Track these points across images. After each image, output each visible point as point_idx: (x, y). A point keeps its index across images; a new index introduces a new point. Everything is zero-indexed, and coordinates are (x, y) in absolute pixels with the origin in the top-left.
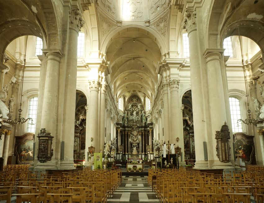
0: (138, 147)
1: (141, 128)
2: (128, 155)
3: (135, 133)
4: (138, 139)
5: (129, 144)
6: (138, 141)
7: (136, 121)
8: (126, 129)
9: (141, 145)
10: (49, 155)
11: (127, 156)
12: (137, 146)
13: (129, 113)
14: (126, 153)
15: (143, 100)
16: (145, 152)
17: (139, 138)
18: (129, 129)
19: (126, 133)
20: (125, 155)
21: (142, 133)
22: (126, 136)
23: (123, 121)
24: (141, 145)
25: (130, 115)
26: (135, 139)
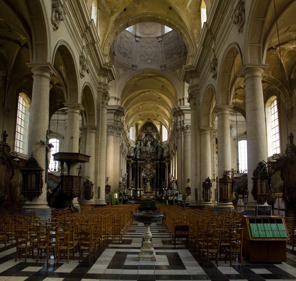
2: (140, 191)
3: (149, 166)
4: (152, 173)
5: (141, 178)
6: (152, 175)
7: (150, 153)
9: (155, 180)
11: (138, 192)
12: (151, 181)
13: (142, 143)
14: (138, 189)
15: (159, 129)
18: (142, 162)
19: (138, 167)
20: (136, 191)
21: (157, 166)
23: (134, 153)
24: (155, 180)
25: (144, 146)
26: (149, 173)
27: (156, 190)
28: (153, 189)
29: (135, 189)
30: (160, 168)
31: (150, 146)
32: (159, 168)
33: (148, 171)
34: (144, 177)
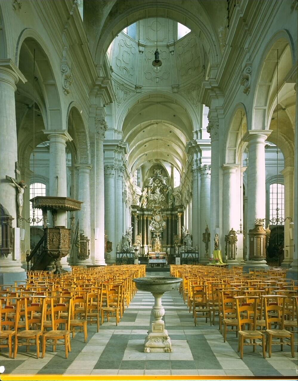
1: (167, 211)
3: (158, 218)
7: (159, 202)
8: (145, 213)
10: (87, 255)
12: (160, 236)
13: (149, 191)
17: (163, 225)
18: (149, 213)
19: (145, 219)
21: (168, 218)
22: (145, 222)
23: (140, 202)
25: (151, 193)
26: (158, 227)
27: (167, 247)
30: (172, 220)
31: (159, 193)
32: (169, 220)
33: (157, 223)
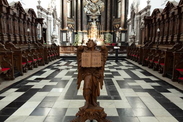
0: (100, 22)
6: (99, 12)
9: (103, 19)
14: (80, 31)
16: (111, 29)
17: (101, 7)
24: (103, 19)
26: (94, 9)
28: (100, 31)
29: (75, 31)
33: (94, 5)
34: (87, 13)
